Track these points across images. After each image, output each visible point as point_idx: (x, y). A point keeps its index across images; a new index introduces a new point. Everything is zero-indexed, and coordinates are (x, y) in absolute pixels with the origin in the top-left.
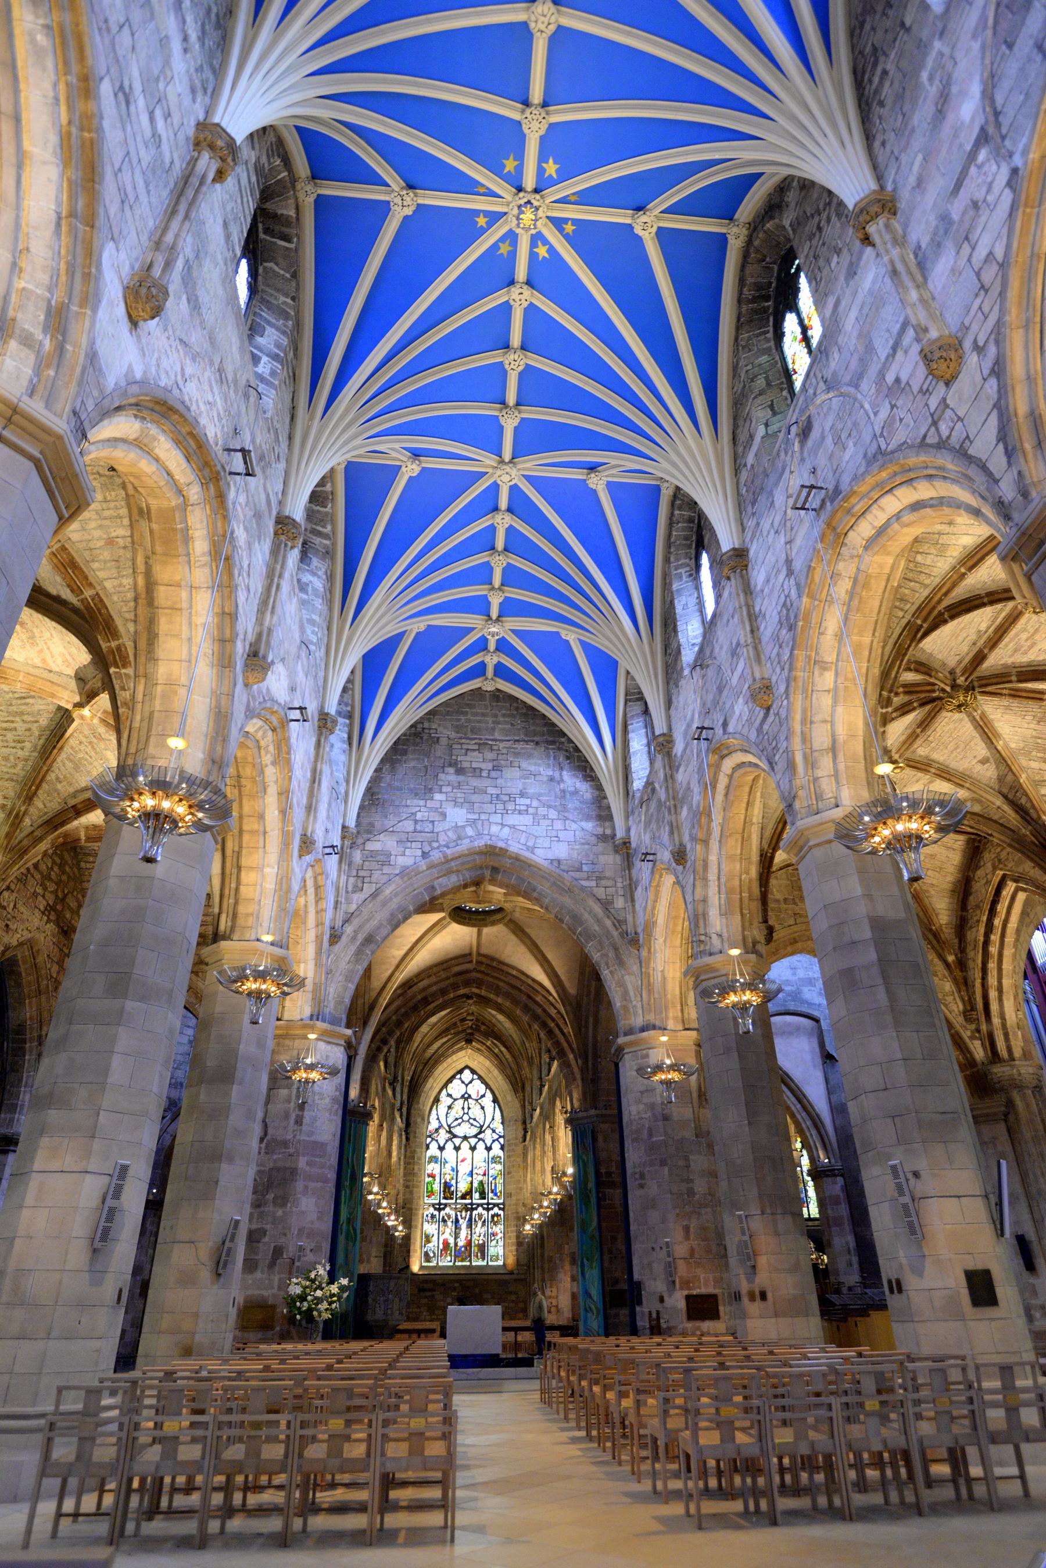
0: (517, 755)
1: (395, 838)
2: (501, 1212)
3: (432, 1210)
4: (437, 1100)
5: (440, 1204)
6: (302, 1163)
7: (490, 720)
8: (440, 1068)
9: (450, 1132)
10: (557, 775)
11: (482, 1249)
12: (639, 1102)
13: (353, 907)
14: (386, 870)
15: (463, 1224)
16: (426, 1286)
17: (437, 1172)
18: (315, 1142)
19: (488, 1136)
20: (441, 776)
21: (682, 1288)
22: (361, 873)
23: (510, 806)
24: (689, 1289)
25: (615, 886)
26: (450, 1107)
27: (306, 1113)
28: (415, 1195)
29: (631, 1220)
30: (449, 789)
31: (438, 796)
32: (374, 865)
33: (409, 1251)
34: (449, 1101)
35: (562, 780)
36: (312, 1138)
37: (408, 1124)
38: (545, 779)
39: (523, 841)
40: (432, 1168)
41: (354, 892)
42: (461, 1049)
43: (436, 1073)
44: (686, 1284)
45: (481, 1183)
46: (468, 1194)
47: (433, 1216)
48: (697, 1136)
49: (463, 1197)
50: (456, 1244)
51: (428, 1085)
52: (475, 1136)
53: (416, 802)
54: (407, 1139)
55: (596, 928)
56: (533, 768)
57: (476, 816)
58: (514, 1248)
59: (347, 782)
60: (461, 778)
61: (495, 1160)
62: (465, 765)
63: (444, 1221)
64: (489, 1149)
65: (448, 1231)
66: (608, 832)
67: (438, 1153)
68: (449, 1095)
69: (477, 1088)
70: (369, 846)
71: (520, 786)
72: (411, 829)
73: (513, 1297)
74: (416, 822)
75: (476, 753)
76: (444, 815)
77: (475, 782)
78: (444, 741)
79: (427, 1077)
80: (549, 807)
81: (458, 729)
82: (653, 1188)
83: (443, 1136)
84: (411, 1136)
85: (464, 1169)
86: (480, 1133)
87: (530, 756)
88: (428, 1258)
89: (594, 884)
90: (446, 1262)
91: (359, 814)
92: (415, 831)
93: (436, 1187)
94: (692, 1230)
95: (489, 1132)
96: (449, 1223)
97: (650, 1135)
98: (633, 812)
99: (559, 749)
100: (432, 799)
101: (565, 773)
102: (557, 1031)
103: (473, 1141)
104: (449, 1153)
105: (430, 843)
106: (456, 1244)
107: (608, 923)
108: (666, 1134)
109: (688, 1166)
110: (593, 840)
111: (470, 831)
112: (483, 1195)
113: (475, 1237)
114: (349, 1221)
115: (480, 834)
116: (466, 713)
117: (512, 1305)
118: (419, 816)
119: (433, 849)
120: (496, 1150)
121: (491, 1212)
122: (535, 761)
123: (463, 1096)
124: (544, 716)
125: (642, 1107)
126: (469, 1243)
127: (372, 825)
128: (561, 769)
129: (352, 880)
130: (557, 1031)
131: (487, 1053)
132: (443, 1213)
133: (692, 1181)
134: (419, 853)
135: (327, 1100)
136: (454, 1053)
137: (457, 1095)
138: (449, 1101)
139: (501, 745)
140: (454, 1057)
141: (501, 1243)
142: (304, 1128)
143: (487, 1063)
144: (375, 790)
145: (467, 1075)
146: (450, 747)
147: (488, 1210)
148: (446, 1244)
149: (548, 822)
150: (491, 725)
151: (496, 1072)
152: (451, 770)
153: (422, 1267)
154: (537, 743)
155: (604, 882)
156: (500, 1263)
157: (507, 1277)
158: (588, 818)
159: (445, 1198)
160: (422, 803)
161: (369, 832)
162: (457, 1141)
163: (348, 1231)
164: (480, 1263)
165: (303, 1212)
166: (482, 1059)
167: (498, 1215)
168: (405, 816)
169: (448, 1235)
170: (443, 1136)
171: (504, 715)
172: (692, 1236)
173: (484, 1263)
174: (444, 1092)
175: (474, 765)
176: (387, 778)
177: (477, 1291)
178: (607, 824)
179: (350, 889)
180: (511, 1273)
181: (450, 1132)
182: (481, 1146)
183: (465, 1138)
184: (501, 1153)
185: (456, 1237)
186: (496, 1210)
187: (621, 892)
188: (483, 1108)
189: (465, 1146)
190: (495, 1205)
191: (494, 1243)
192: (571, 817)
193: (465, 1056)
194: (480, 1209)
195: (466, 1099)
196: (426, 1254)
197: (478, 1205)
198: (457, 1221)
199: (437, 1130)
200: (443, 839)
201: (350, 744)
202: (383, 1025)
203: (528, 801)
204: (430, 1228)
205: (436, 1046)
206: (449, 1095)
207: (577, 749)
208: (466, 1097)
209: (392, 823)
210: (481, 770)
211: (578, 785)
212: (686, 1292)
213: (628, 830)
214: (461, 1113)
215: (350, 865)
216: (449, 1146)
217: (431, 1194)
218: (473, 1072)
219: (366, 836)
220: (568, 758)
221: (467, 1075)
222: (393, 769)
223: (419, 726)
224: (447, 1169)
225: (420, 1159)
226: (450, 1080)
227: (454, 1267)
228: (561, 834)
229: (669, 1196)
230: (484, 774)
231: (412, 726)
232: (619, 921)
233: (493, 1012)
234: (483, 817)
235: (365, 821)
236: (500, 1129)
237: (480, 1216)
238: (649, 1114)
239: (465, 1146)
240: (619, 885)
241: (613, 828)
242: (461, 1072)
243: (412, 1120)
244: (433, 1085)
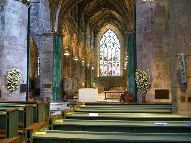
2: (119, 64)
3: (102, 63)
4: (102, 37)
5: (104, 62)
6: (6, 43)
8: (102, 29)
9: (106, 45)
11: (114, 72)
12: (141, 17)
15: (110, 66)
16: (101, 80)
17: (103, 55)
18: (11, 36)
19: (116, 46)
21: (154, 87)
24: (157, 87)
26: (105, 39)
27: (6, 26)
28: (97, 60)
29: (137, 63)
33: (96, 72)
34: (105, 37)
36: (10, 35)
37: (94, 43)
40: (101, 54)
42: (107, 24)
43: (101, 30)
44: (156, 86)
45: (114, 57)
46: (111, 59)
47: (102, 65)
48: (166, 30)
49: (110, 60)
50: (108, 71)
51: (99, 34)
52: (112, 46)
54: (94, 47)
58: (122, 72)
61: (117, 51)
63: (105, 66)
64: (116, 49)
65: (106, 68)
67: (102, 50)
68: (105, 36)
69: (113, 34)
73: (122, 83)
79: (99, 32)
82: (145, 51)
83: (104, 46)
84: (95, 46)
85: (110, 54)
86: (113, 45)
88: (101, 74)
90: (106, 75)
93: (103, 58)
94: (160, 66)
95: (116, 45)
96: (106, 66)
97: (146, 29)
102: (123, 7)
103: (112, 47)
104: (106, 50)
106: (108, 71)
108: (152, 29)
109: (161, 42)
112: (115, 60)
113: (113, 69)
114: (57, 64)
117: (122, 84)
120: (118, 49)
121: (117, 64)
123: (109, 36)
125: (143, 19)
126: (111, 72)
130: (123, 7)
131: (114, 25)
132: (104, 64)
133: (162, 47)
135: (16, 22)
136: (106, 25)
137: (107, 36)
138: (105, 37)
140: (106, 26)
141: (119, 71)
142: (5, 31)
143: (115, 27)
145: (110, 31)
147: (116, 63)
148: (106, 71)
151: (117, 30)
153: (100, 76)
156: (119, 75)
157: (121, 78)
159: (105, 61)
162: (108, 47)
163: (57, 66)
164: (114, 75)
165: (8, 61)
166: (113, 26)
167: (118, 65)
169: (106, 69)
170: (104, 46)
172: (160, 68)
173: (115, 75)
174: (104, 35)
177: (113, 81)
180: (122, 77)
181: (106, 45)
182: (114, 48)
183: (110, 46)
184: (119, 50)
185: (108, 69)
186: (118, 63)
188: (114, 39)
189: (110, 48)
190: (118, 62)
191: (118, 71)
193: (108, 26)
194: (114, 63)
195: (110, 37)
196: (101, 73)
197: (113, 62)
198: (108, 66)
199: (102, 45)
202: (64, 7)
204: (101, 67)
205: (100, 22)
206: (105, 36)
208: (110, 36)
212: (156, 89)
214: (108, 40)
216: (106, 48)
217: (101, 59)
218: (111, 30)
221: (110, 31)
224: (105, 54)
225: (98, 52)
226: (105, 32)
227: (108, 76)
229: (151, 53)
233: (114, 12)
236: (119, 44)
237: (114, 65)
238: (146, 21)
239: (110, 48)
242: (108, 30)
243: (95, 42)
244: (100, 34)
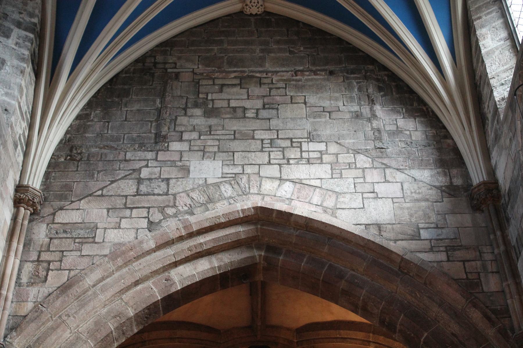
0: (300, 88)
1: (106, 204)
7: (258, 49)
10: (366, 110)
13: (30, 305)
14: (87, 250)
20: (183, 120)
22: (45, 256)
23: (294, 154)
25: (480, 257)
30: (195, 135)
31: (175, 146)
32: (68, 244)
35: (374, 116)
38: (348, 116)
39: (316, 199)
41: (31, 284)
53: (140, 154)
55: (455, 328)
56: (326, 104)
57: (238, 170)
59: (31, 127)
60: (213, 121)
62: (219, 104)
66: (458, 182)
70: (62, 217)
71: (308, 127)
72: (132, 190)
74: (140, 181)
75: (237, 89)
76: (186, 170)
77: (236, 125)
78: (186, 77)
80: (357, 152)
81: (208, 61)
87: (320, 89)
89: (442, 257)
91: (47, 175)
92: (138, 193)
98: (497, 138)
99: (366, 78)
100: (167, 149)
101: (378, 108)
105: (162, 210)
107: (476, 315)
110: (433, 194)
111: (227, 190)
115: (245, 193)
116: (221, 42)
118: (145, 173)
119: (166, 217)
122: (326, 95)
124: (339, 40)
127: (68, 188)
128: (372, 102)
129: (29, 267)
134: (144, 223)
139: (275, 78)
144: (77, 142)
146: (197, 84)
149: (354, 173)
150: (258, 53)
152: (198, 112)
154: (331, 73)
155: (459, 254)
158: (422, 165)
160: (150, 155)
161: (62, 197)
168: (122, 174)
171: (278, 42)
175: (233, 104)
176: (97, 126)
178: (454, 171)
179: (24, 280)
187: (491, 267)
192: (393, 164)
200: (183, 201)
201: (37, 74)
203: (322, 147)
207: (393, 77)
209: (101, 185)
210: (245, 109)
211: (401, 122)
213: (492, 172)
215: (27, 245)
219: (57, 204)
220: (380, 89)
222: (106, 117)
223: (149, 62)
228: (380, 189)
230: (250, 114)
231: (137, 61)
232: (494, 311)
234: (249, 170)
235: (57, 184)
240: (488, 257)
241: (466, 176)
